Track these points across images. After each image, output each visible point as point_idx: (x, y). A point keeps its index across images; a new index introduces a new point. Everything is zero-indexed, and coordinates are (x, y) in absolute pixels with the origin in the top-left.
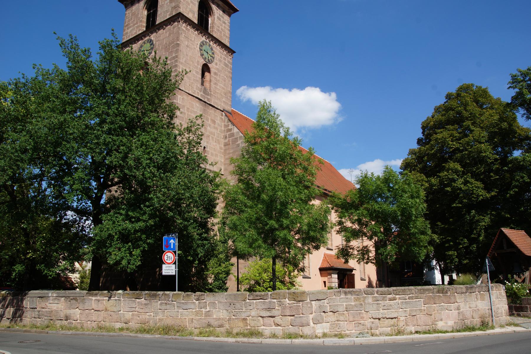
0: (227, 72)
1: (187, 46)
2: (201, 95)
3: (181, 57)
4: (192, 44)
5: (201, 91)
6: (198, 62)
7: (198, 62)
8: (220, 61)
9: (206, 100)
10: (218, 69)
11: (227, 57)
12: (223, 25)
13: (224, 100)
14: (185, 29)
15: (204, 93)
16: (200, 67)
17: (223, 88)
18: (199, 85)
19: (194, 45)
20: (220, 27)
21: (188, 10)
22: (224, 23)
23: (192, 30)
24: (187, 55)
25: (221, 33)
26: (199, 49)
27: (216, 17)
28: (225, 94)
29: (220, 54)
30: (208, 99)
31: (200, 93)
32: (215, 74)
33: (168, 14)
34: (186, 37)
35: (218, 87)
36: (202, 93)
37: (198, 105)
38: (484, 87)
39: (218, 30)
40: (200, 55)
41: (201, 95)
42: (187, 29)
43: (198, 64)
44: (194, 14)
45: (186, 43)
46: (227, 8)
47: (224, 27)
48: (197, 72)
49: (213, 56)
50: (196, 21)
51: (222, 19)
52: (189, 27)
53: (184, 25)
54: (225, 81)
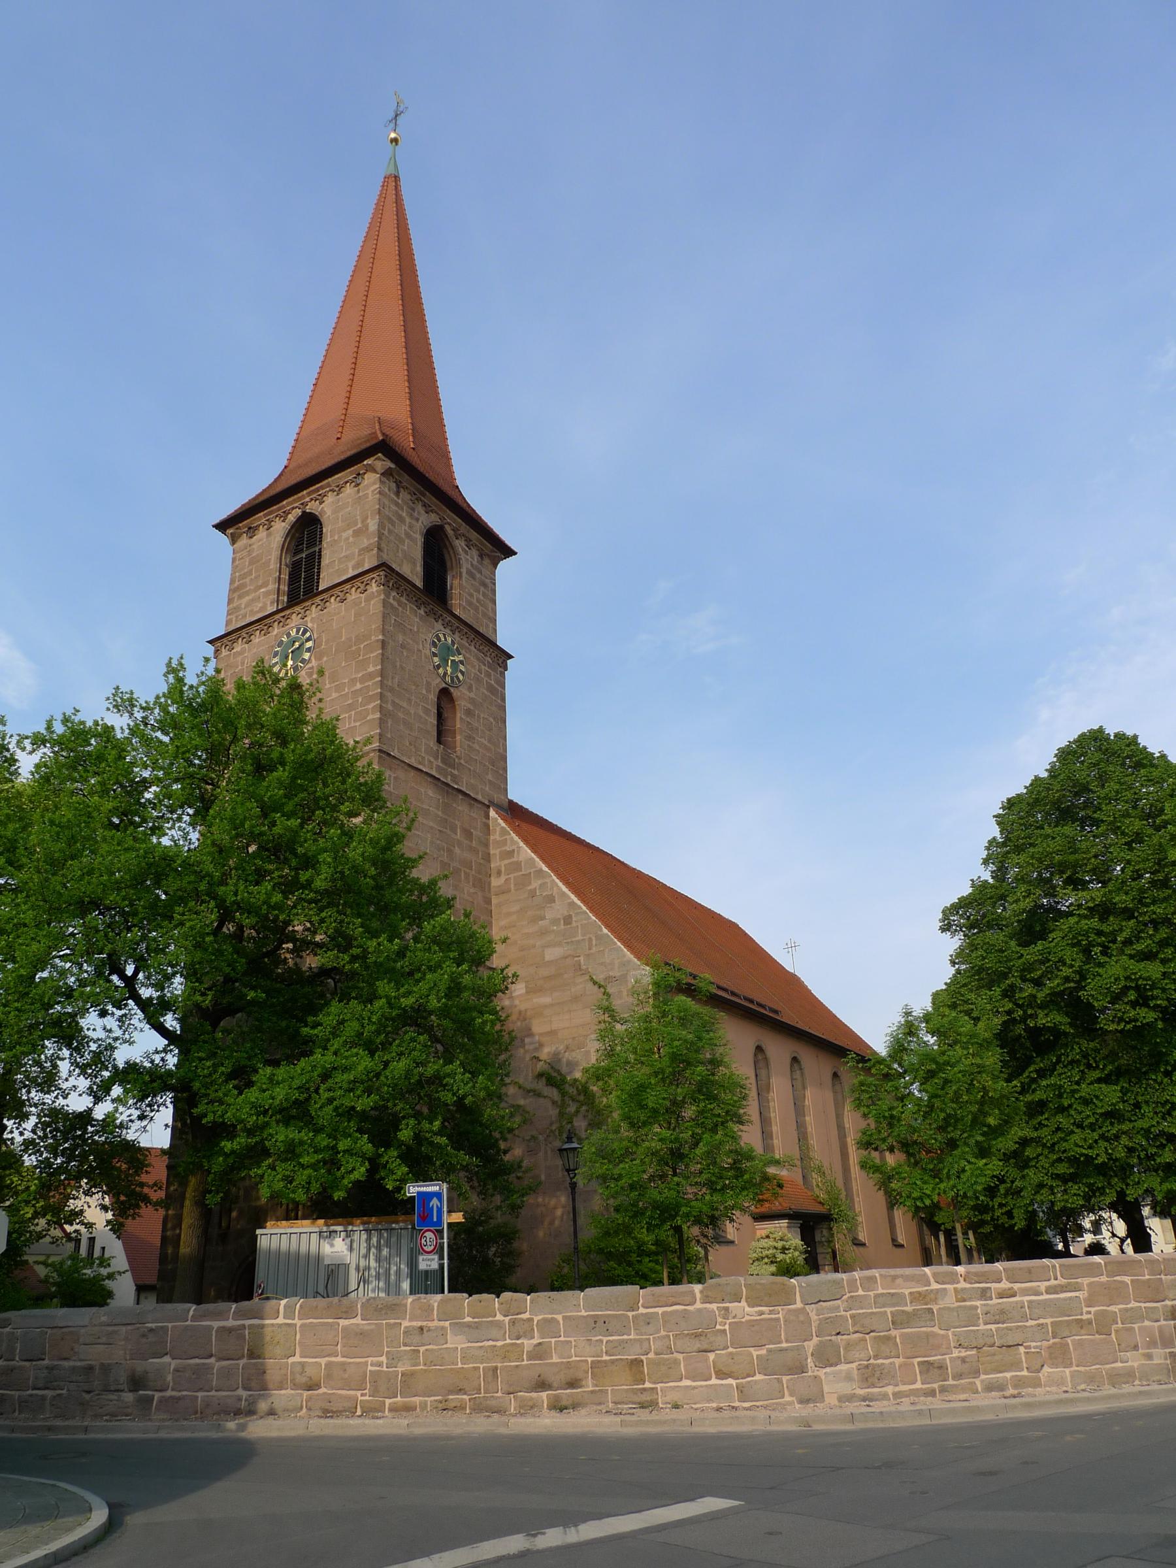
5: (436, 758)
6: (428, 683)
7: (428, 683)
9: (449, 780)
10: (472, 701)
12: (482, 589)
13: (490, 777)
14: (395, 604)
15: (444, 761)
16: (433, 697)
18: (432, 743)
19: (417, 643)
24: (402, 668)
25: (476, 609)
27: (464, 571)
29: (476, 663)
31: (435, 763)
33: (350, 564)
35: (476, 746)
37: (430, 793)
38: (1130, 733)
39: (470, 604)
41: (438, 768)
43: (429, 691)
44: (414, 564)
48: (427, 711)
51: (478, 575)
54: (490, 730)
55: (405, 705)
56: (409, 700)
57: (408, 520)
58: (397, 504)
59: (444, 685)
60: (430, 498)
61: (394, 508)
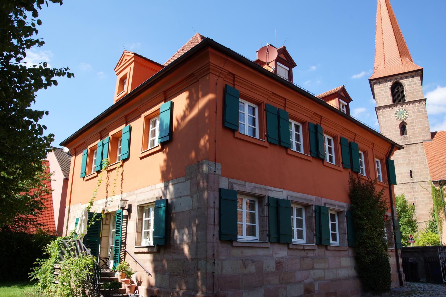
2: (402, 142)
10: (413, 119)
13: (422, 135)
15: (404, 139)
22: (415, 84)
23: (388, 109)
24: (386, 126)
25: (413, 92)
28: (423, 130)
29: (413, 109)
30: (408, 142)
32: (412, 123)
35: (416, 130)
36: (403, 141)
42: (383, 112)
45: (385, 120)
46: (414, 73)
47: (416, 87)
49: (407, 113)
50: (391, 102)
52: (384, 110)
53: (381, 110)
55: (389, 134)
56: (390, 132)
57: (384, 89)
58: (380, 88)
60: (389, 79)
61: (379, 89)
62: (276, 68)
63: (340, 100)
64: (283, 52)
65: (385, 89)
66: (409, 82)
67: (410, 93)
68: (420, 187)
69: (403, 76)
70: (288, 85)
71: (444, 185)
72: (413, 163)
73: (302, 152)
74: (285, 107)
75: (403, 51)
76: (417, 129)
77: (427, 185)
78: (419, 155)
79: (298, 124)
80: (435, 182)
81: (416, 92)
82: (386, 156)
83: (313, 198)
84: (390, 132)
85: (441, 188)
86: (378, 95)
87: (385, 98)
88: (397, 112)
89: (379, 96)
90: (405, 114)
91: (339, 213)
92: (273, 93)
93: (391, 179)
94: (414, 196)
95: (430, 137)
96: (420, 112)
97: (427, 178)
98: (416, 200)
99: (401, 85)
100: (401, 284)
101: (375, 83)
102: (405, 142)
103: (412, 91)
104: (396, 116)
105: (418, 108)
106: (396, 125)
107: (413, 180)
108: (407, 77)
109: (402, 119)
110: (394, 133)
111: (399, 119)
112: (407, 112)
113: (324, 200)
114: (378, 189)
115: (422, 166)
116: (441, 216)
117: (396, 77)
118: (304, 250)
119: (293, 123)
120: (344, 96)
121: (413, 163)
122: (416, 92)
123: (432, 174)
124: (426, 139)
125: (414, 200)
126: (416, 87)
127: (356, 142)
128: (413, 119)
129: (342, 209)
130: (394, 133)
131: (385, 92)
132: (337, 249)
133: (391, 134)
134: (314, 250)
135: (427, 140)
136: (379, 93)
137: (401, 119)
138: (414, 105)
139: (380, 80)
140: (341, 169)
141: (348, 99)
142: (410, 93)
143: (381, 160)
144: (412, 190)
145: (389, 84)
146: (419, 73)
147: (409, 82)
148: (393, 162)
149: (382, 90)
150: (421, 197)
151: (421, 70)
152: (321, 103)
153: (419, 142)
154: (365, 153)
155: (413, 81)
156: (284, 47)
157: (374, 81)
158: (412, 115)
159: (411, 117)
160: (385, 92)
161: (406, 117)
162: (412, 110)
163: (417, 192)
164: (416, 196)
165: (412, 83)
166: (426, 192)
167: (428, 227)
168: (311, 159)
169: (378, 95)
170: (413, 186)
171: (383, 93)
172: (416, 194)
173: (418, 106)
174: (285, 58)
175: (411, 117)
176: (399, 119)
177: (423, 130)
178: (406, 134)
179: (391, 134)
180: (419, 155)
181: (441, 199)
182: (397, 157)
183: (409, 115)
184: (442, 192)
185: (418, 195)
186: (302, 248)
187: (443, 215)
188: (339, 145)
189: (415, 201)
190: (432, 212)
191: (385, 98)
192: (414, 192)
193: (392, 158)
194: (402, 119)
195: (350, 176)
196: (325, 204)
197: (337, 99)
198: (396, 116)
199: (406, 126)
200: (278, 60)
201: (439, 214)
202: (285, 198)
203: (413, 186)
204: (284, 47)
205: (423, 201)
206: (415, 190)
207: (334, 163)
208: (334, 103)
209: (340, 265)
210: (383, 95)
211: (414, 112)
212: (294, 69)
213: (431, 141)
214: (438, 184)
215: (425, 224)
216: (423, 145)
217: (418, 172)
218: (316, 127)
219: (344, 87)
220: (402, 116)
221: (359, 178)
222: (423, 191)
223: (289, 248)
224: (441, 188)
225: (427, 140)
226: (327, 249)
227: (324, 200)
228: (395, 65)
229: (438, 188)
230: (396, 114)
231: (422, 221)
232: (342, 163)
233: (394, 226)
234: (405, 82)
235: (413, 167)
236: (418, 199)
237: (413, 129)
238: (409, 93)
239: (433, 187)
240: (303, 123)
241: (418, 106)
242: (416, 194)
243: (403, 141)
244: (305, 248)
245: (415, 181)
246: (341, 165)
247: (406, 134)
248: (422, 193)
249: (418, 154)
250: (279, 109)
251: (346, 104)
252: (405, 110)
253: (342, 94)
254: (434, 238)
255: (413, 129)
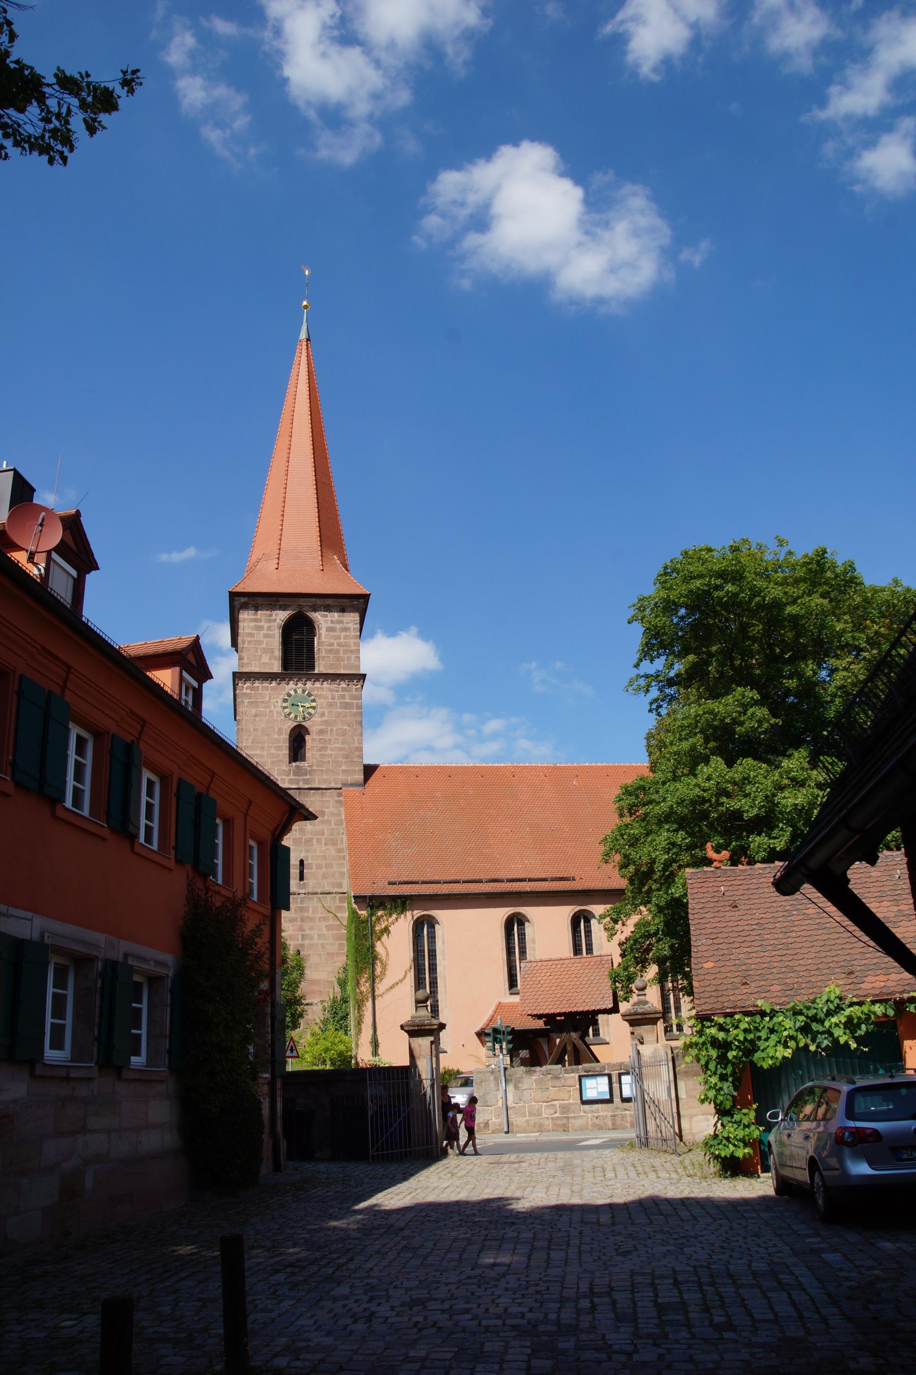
0: (349, 718)
1: (255, 716)
2: (291, 781)
3: (245, 737)
4: (265, 707)
7: (280, 730)
8: (331, 705)
9: (301, 785)
10: (326, 723)
11: (350, 690)
13: (344, 767)
14: (248, 691)
15: (295, 774)
16: (285, 737)
17: (340, 749)
19: (269, 707)
20: (335, 642)
21: (259, 653)
22: (346, 629)
23: (266, 684)
24: (256, 730)
26: (280, 709)
28: (347, 757)
29: (329, 694)
30: (306, 781)
31: (287, 778)
32: (321, 732)
34: (252, 702)
35: (329, 752)
36: (292, 777)
40: (283, 718)
42: (252, 689)
45: (253, 711)
49: (314, 704)
50: (277, 667)
52: (257, 684)
53: (248, 684)
55: (259, 752)
56: (263, 748)
57: (266, 625)
58: (255, 620)
59: (296, 724)
61: (252, 624)
62: (47, 569)
63: (185, 674)
64: (73, 524)
65: (269, 628)
66: (332, 622)
67: (330, 651)
68: (320, 909)
69: (319, 602)
70: (69, 619)
71: (378, 908)
72: (309, 841)
73: (86, 812)
74: (64, 688)
75: (330, 537)
76: (331, 749)
77: (338, 904)
78: (329, 822)
79: (85, 734)
80: (359, 899)
81: (345, 652)
82: (273, 834)
83: (100, 938)
84: (263, 748)
85: (371, 915)
86: (247, 639)
87: (265, 651)
88: (289, 695)
89: (249, 642)
90: (307, 705)
91: (154, 980)
92: (44, 649)
93: (278, 896)
94: (301, 929)
95: (360, 777)
96: (345, 708)
97: (340, 886)
98: (307, 942)
99: (310, 627)
100: (277, 1167)
101: (245, 606)
102: (298, 782)
103: (335, 647)
104: (285, 708)
105: (343, 697)
106: (280, 731)
107: (304, 886)
108: (328, 609)
109: (300, 719)
110: (273, 751)
111: (292, 716)
112: (313, 701)
113: (125, 946)
114: (251, 922)
115: (332, 850)
116: (363, 989)
117: (302, 601)
118: (68, 1079)
119: (75, 731)
120: (194, 663)
121: (309, 841)
122: (345, 652)
123: (354, 875)
124: (350, 779)
125: (300, 942)
126: (346, 637)
127: (212, 795)
128: (326, 721)
129: (162, 971)
130: (273, 751)
131: (266, 636)
132: (143, 1078)
133: (265, 753)
134: (90, 1079)
135: (352, 785)
136: (251, 635)
137: (296, 717)
138: (334, 686)
139: (259, 600)
140: (171, 864)
141: (203, 674)
142: (330, 651)
143: (260, 844)
144: (298, 915)
145: (282, 616)
146: (357, 603)
147: (332, 622)
148: (287, 850)
149: (260, 628)
150: (319, 935)
151: (366, 597)
152: (134, 669)
153: (333, 785)
154: (228, 823)
155: (341, 622)
156: (78, 514)
157: (243, 600)
158: (326, 711)
159: (322, 715)
160: (266, 636)
161: (310, 714)
162: (327, 698)
163: (311, 919)
164: (307, 932)
165: (338, 626)
166: (331, 922)
167: (328, 1015)
168: (106, 833)
169: (247, 639)
170: (301, 903)
171: (260, 636)
172: (307, 925)
173: (344, 690)
174: (77, 550)
175: (322, 715)
176: (292, 716)
177: (347, 757)
178: (303, 759)
179: (265, 753)
180: (329, 822)
181: (368, 944)
182: (298, 840)
183: (319, 710)
184: (373, 927)
185: (312, 929)
186: (63, 1073)
187: (367, 985)
188: (174, 800)
189: (303, 945)
190: (342, 976)
191: (265, 651)
192: (302, 920)
193: (287, 841)
194: (300, 719)
195: (189, 885)
196: (126, 956)
197: (177, 669)
198: (285, 708)
199: (307, 738)
200: (61, 549)
201: (358, 984)
202: (36, 936)
203: (301, 903)
204: (78, 514)
205: (323, 947)
206: (306, 914)
207: (155, 847)
208: (165, 678)
209: (144, 1121)
210: (260, 643)
211: (331, 705)
212: (91, 579)
213: (361, 789)
214: (365, 905)
215: (320, 1007)
216: (340, 795)
217: (319, 867)
218: (129, 749)
219: (198, 638)
220: (301, 709)
221: (207, 889)
222: (325, 919)
223: (32, 1075)
224: (371, 915)
225: (352, 785)
226: (119, 1077)
227: (125, 946)
228: (305, 572)
229: (364, 913)
230: (285, 701)
231: (315, 1001)
232: (176, 848)
233: (273, 1018)
234: (323, 620)
235: (307, 851)
236: (311, 938)
237: (322, 749)
238: (327, 651)
239: (353, 912)
240: (98, 735)
241: (344, 690)
242: (307, 925)
243: (292, 777)
244: (72, 1075)
245: (310, 890)
246: (173, 852)
247: (303, 759)
248: (323, 924)
249: (326, 818)
250: (50, 692)
251: (196, 684)
252: (309, 695)
253: (191, 657)
254: (342, 1047)
255: (322, 749)
